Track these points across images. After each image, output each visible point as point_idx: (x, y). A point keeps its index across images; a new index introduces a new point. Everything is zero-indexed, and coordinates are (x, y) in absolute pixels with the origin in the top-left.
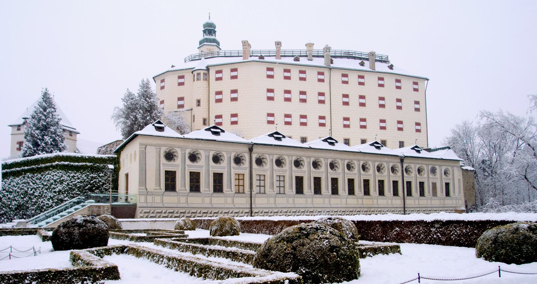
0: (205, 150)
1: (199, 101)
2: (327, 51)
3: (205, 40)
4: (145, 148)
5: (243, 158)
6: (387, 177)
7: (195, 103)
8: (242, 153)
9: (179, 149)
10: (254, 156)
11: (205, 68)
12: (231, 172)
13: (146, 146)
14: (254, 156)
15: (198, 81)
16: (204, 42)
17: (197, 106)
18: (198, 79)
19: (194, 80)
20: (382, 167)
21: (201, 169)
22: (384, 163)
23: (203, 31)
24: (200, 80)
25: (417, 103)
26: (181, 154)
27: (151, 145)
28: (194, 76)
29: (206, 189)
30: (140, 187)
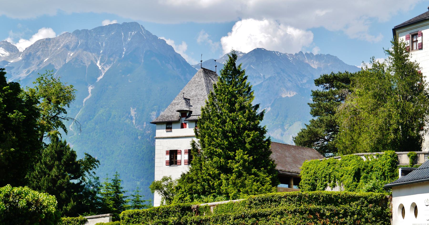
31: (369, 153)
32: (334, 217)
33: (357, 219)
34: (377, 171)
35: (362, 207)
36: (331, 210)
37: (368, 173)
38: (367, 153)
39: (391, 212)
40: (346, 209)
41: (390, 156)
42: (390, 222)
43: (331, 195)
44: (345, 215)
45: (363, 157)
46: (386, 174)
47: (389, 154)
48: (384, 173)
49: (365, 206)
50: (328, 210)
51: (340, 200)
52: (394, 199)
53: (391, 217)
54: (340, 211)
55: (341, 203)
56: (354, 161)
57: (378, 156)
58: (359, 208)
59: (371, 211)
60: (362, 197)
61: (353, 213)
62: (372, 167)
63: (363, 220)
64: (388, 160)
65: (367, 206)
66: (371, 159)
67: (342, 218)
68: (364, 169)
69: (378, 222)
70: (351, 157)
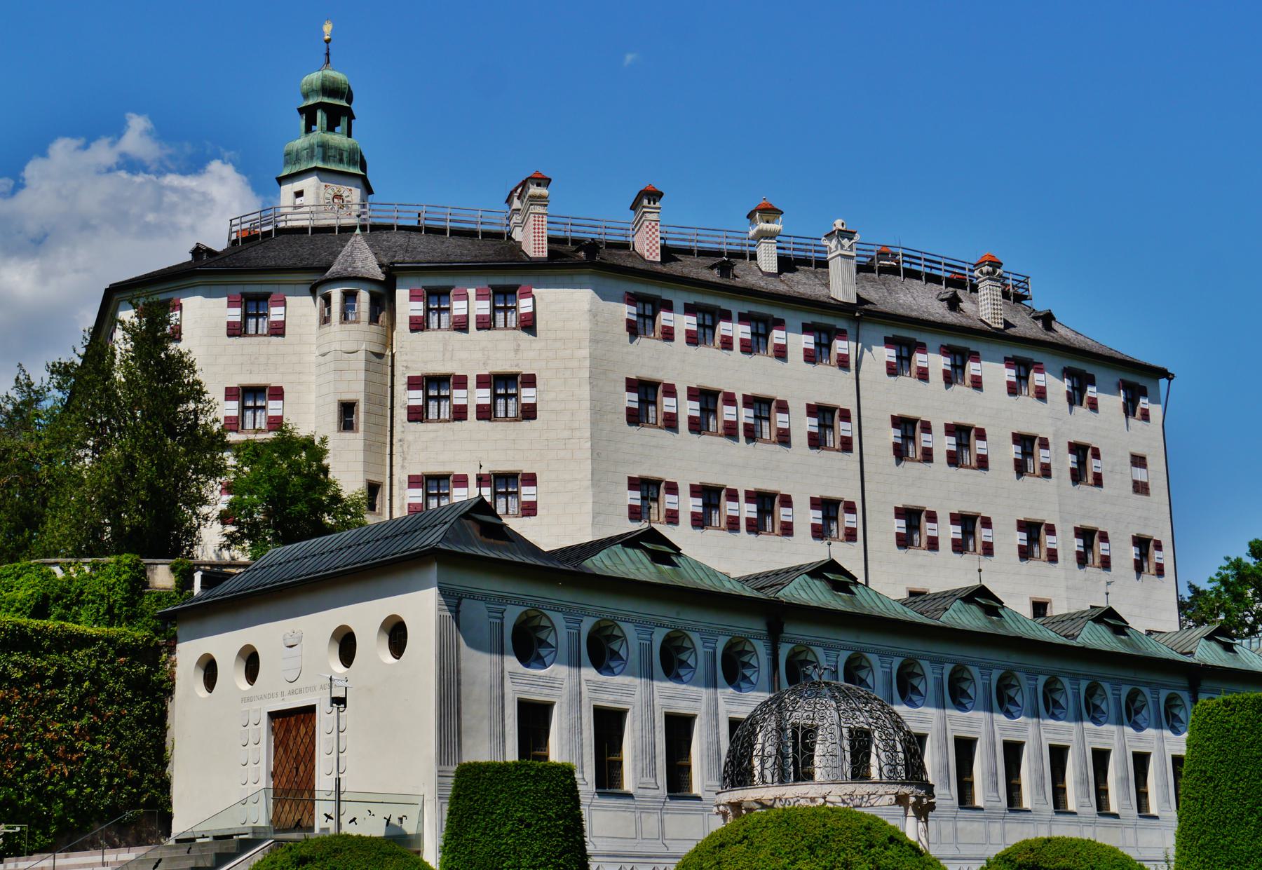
0: (637, 623)
1: (347, 410)
2: (842, 246)
3: (318, 151)
4: (459, 604)
5: (745, 659)
6: (1155, 742)
7: (332, 416)
8: (746, 640)
9: (560, 615)
10: (784, 651)
11: (382, 277)
12: (717, 715)
13: (460, 599)
14: (784, 651)
15: (348, 327)
16: (311, 157)
17: (339, 431)
18: (345, 318)
19: (325, 320)
20: (1138, 704)
21: (629, 699)
22: (1143, 689)
23: (301, 111)
24: (357, 322)
25: (1139, 461)
26: (565, 636)
27: (474, 597)
28: (327, 299)
29: (644, 780)
30: (443, 768)
31: (73, 561)
32: (29, 684)
33: (88, 692)
34: (94, 602)
35: (102, 662)
36: (24, 667)
37: (67, 607)
38: (69, 560)
39: (173, 680)
40: (61, 667)
41: (129, 566)
42: (164, 704)
43: (25, 628)
44: (59, 680)
45: (57, 569)
46: (116, 611)
47: (128, 561)
48: (110, 610)
49: (109, 662)
50: (15, 664)
51: (46, 643)
52: (179, 647)
53: (170, 692)
54: (48, 670)
55: (49, 651)
56: (32, 578)
57: (95, 567)
58: (93, 664)
59: (121, 674)
60: (101, 638)
61: (79, 679)
62: (82, 593)
63: (103, 696)
64: (124, 576)
65: (112, 661)
66: (78, 572)
67: (51, 687)
68: (59, 598)
69: (138, 703)
70: (22, 569)
